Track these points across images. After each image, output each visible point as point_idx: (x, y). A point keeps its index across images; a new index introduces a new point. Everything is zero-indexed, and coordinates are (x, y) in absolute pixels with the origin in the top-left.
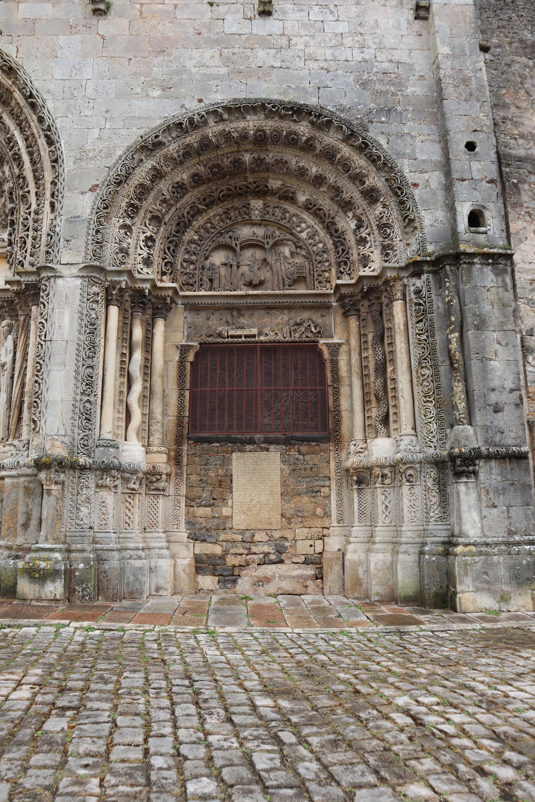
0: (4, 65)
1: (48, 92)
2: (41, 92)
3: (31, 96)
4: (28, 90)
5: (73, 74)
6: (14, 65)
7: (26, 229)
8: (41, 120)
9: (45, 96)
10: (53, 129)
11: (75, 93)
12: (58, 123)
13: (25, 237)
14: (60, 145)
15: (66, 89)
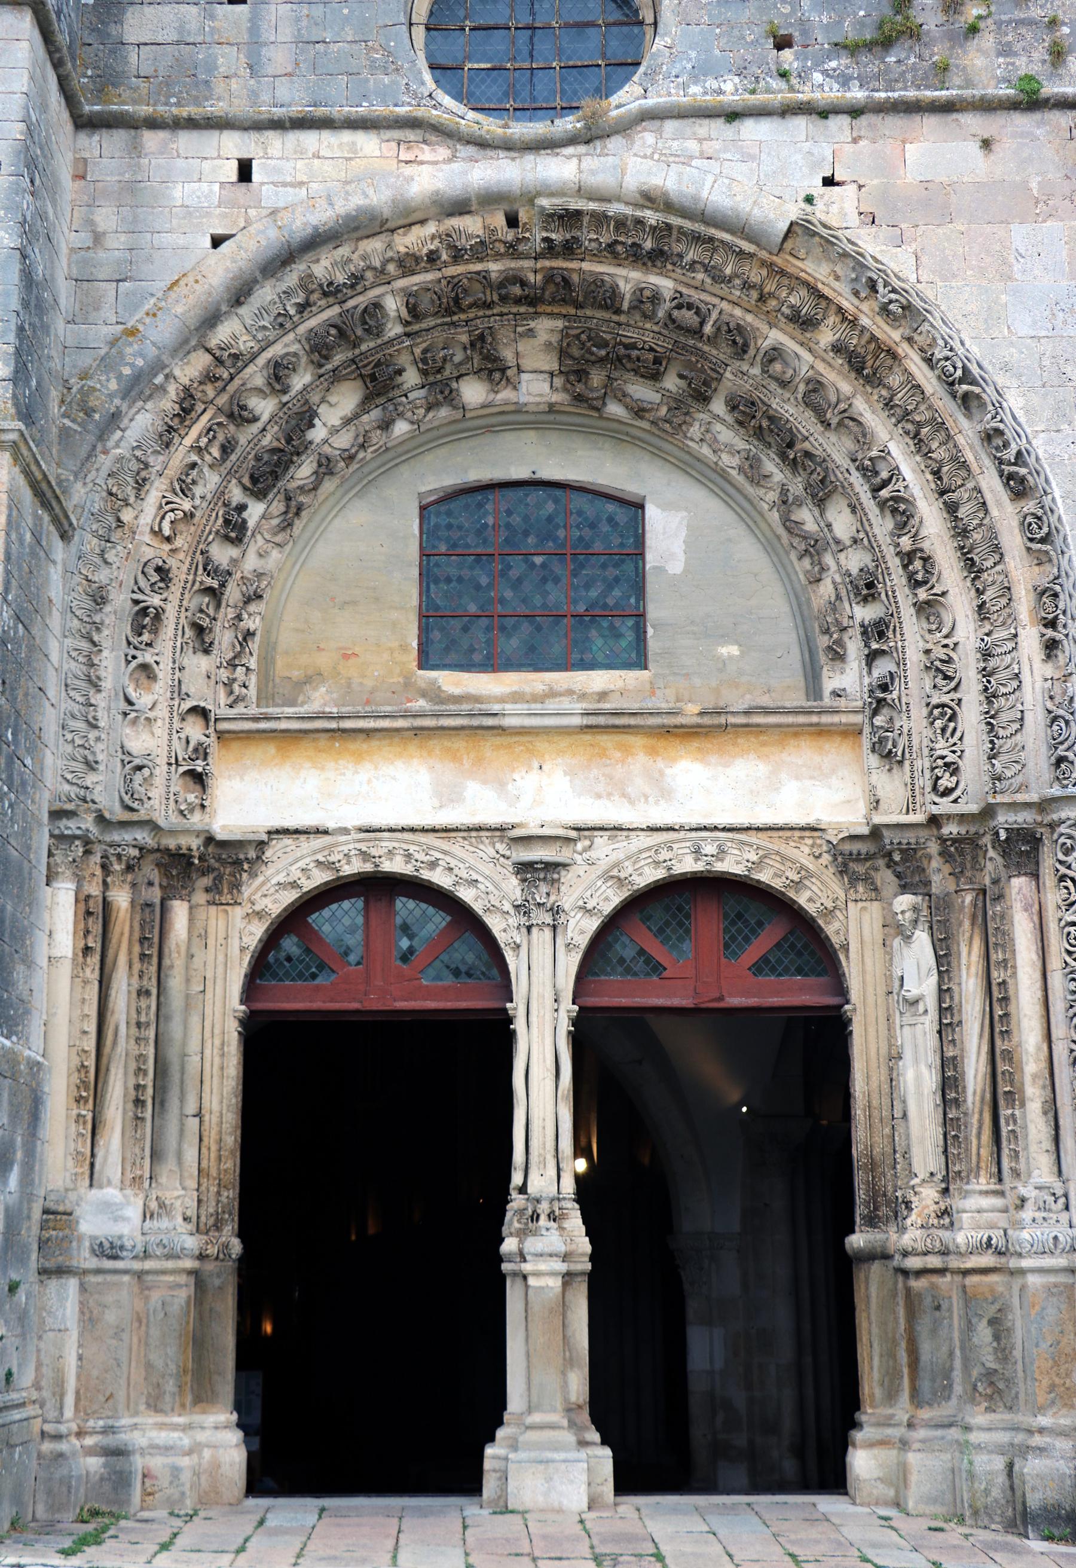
0: (891, 302)
1: (1006, 368)
2: (989, 368)
3: (967, 377)
4: (959, 365)
5: (1059, 323)
6: (917, 303)
7: (953, 684)
8: (992, 437)
9: (1001, 380)
10: (1032, 461)
11: (1068, 369)
12: (1041, 446)
13: (952, 704)
14: (1053, 499)
15: (1046, 362)
